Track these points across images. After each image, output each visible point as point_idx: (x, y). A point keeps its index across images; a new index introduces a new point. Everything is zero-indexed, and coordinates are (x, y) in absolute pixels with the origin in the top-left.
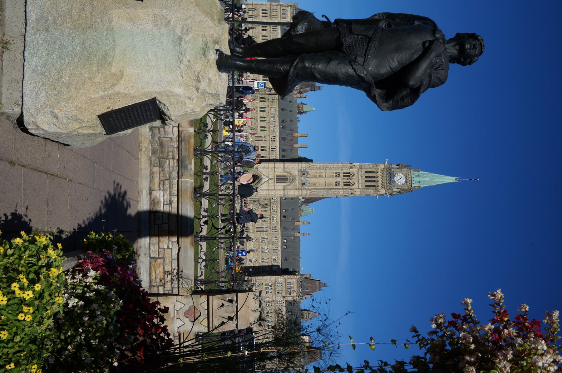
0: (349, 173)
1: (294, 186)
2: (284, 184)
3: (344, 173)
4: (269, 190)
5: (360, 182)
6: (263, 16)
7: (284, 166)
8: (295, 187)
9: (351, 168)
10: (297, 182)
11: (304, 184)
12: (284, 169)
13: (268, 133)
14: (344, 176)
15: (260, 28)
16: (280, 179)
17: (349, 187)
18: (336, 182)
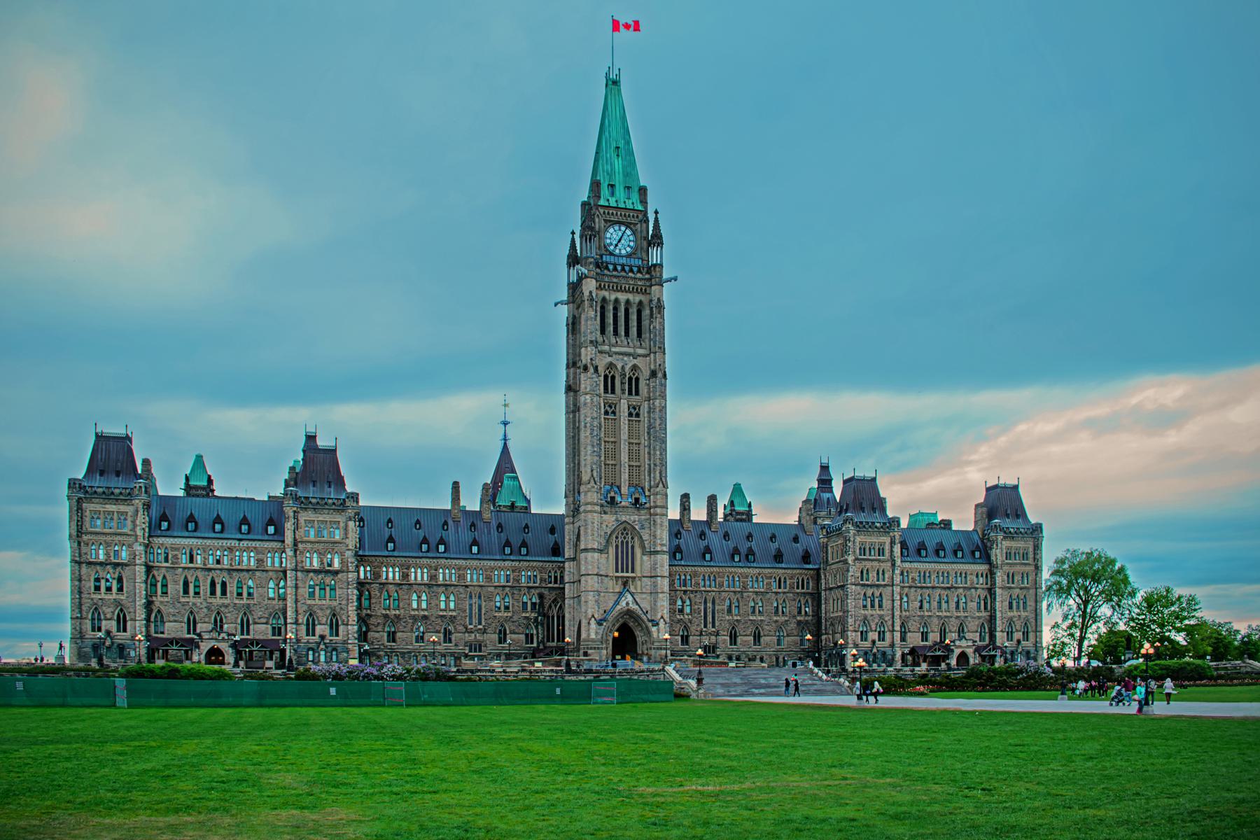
0: (606, 377)
1: (642, 527)
2: (638, 551)
3: (606, 391)
4: (654, 593)
5: (631, 350)
6: (120, 589)
7: (593, 550)
8: (647, 525)
9: (596, 369)
10: (633, 518)
11: (637, 500)
12: (600, 551)
13: (461, 590)
14: (613, 392)
15: (158, 600)
16: (625, 561)
17: (642, 384)
18: (630, 415)
